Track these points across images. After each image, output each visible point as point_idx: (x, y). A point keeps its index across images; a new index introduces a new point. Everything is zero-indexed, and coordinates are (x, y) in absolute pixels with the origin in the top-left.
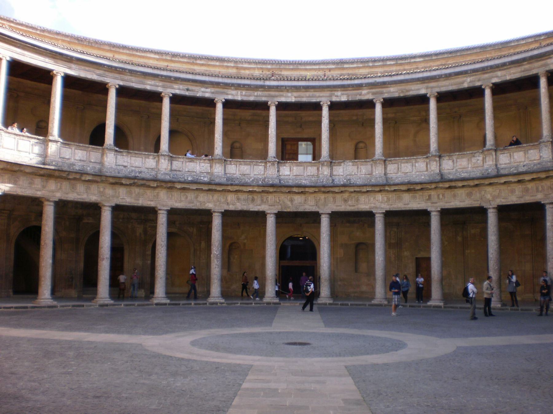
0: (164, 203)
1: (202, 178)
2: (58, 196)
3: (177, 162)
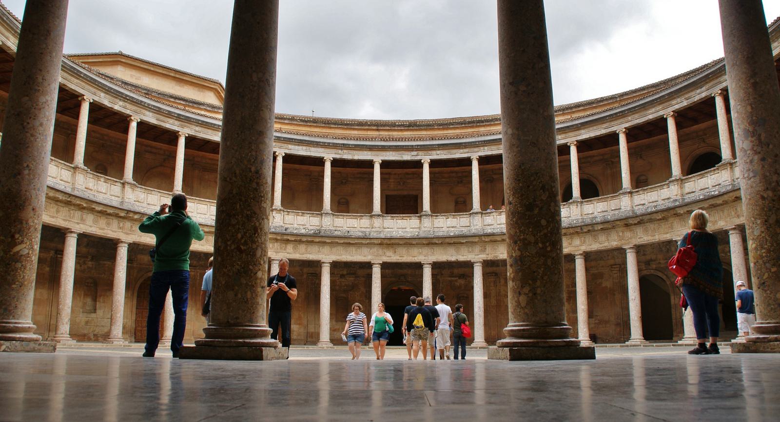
0: (679, 233)
1: (713, 193)
2: (585, 248)
3: (689, 183)
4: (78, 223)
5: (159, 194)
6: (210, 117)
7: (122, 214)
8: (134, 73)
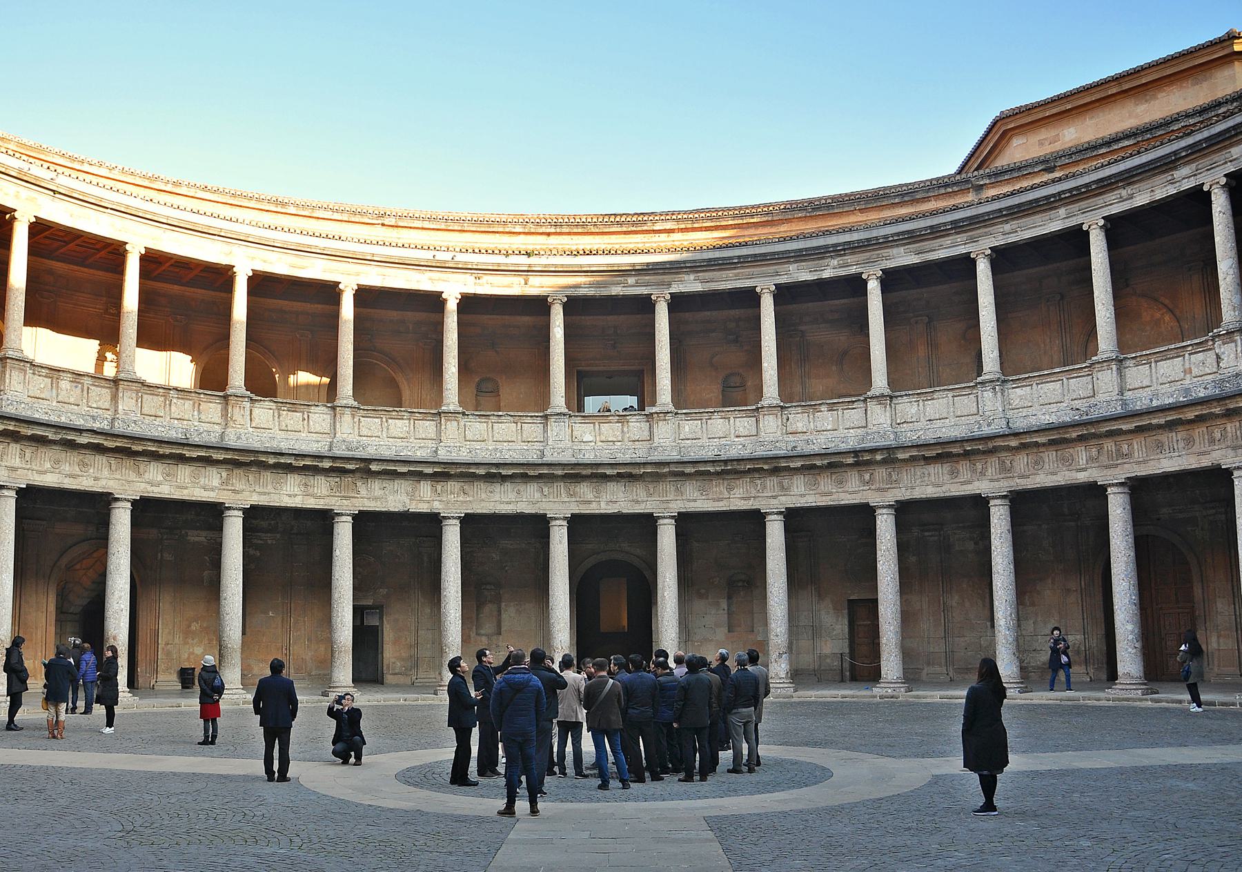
4: (774, 497)
5: (950, 394)
6: (1032, 188)
7: (850, 460)
8: (1044, 134)
